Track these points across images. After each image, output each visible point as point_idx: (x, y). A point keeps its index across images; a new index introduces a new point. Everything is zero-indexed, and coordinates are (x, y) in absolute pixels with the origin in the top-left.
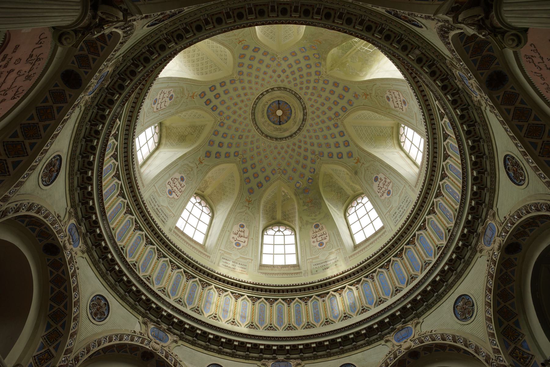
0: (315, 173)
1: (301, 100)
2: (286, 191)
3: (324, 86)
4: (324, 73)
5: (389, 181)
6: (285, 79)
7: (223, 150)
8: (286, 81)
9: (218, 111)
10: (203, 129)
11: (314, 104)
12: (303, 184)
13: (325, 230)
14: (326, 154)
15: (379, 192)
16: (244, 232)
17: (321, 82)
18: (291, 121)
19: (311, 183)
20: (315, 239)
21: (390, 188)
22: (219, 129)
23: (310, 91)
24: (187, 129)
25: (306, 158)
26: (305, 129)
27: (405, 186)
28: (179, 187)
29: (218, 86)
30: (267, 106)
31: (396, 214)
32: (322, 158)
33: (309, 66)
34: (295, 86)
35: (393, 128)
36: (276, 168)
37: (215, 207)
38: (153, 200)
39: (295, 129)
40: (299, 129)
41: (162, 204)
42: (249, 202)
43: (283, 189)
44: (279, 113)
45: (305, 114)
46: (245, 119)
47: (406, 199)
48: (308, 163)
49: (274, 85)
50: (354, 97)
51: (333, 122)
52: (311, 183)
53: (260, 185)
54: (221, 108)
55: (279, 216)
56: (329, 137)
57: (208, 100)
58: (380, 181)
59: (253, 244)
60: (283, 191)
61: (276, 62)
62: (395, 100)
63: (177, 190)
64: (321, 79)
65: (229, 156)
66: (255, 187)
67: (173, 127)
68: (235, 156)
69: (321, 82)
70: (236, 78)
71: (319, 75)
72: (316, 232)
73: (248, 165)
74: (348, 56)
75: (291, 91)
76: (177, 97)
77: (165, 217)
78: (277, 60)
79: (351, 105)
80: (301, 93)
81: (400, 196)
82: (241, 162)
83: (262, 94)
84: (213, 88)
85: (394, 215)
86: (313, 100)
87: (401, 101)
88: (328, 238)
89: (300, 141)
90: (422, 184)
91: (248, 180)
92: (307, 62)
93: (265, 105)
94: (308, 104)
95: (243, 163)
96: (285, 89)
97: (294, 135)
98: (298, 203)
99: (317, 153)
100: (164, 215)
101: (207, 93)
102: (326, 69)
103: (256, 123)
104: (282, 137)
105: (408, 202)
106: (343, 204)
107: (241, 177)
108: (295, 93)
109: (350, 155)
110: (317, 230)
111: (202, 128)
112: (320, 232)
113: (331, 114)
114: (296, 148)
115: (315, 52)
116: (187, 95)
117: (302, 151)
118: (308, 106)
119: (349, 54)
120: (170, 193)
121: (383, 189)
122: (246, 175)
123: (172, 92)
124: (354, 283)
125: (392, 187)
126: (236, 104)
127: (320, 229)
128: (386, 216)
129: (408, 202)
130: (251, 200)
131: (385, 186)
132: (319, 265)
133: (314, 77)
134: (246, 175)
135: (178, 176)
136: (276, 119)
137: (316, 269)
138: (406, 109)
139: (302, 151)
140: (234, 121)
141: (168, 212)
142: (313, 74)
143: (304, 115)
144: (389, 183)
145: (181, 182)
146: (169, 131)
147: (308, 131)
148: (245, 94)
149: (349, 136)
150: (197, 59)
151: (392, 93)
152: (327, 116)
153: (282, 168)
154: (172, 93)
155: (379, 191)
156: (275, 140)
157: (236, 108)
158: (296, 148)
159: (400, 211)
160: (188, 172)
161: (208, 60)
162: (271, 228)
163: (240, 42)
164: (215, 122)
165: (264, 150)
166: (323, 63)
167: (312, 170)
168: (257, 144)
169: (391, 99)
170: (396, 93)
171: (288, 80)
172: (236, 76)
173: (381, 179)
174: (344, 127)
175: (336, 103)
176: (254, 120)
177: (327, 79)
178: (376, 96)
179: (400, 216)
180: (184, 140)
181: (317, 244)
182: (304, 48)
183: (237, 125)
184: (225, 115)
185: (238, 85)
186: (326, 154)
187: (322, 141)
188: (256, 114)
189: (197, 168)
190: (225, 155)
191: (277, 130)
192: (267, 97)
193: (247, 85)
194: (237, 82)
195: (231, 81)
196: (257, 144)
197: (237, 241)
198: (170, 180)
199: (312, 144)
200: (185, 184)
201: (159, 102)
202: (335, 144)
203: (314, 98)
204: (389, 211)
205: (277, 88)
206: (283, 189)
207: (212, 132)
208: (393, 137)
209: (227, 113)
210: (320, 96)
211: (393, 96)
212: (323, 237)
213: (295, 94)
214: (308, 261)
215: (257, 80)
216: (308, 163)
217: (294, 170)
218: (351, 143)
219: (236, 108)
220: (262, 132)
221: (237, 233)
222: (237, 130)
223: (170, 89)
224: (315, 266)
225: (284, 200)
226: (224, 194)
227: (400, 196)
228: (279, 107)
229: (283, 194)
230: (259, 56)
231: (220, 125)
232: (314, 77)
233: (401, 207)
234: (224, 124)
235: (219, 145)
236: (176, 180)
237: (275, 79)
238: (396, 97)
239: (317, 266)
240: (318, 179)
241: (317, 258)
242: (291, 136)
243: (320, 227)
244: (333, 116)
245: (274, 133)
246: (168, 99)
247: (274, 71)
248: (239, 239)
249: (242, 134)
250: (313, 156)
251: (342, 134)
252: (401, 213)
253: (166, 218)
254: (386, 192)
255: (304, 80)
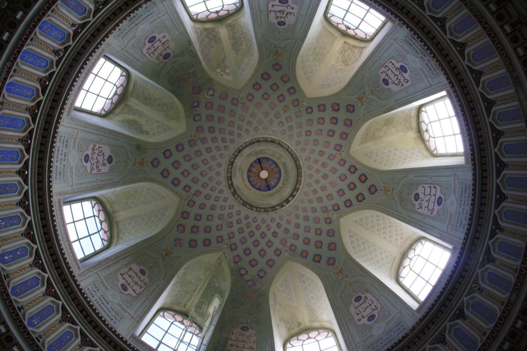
0: (192, 116)
1: (242, 203)
2: (225, 76)
3: (219, 233)
4: (226, 251)
5: (94, 172)
6: (270, 224)
7: (329, 114)
8: (268, 222)
9: (347, 165)
10: (363, 138)
11: (224, 203)
12: (204, 96)
13: (153, 58)
14: (187, 146)
15: (99, 147)
16: (277, 17)
17: (226, 237)
18: (246, 168)
19: (193, 102)
20: (163, 40)
21: (88, 165)
22: (341, 142)
23: (235, 219)
24: (384, 133)
25: (212, 129)
26: (225, 166)
27: (72, 186)
28: (389, 73)
29: (354, 201)
30: (282, 179)
31: (65, 146)
32: (190, 138)
33: (247, 252)
34: (255, 218)
35: (114, 212)
36: (248, 103)
37: (323, 26)
38: (432, 69)
39: (238, 162)
40: (232, 163)
41: (417, 60)
42: (277, 54)
43: (230, 78)
44: (264, 174)
45: (231, 186)
46: (308, 159)
47: (62, 175)
48: (206, 125)
49: (281, 211)
50: (180, 240)
51: (193, 191)
52: (195, 101)
53: (266, 76)
54: (343, 170)
55: (223, 31)
56: (191, 170)
57: (364, 182)
58: (104, 162)
59: (259, 5)
60: (228, 74)
61: (288, 245)
62: (136, 279)
63: (393, 70)
64: (227, 241)
65: (319, 106)
66: (272, 72)
67: (402, 131)
68: (311, 108)
69: (226, 237)
70: (333, 214)
71: (231, 245)
72: (165, 49)
73: (289, 99)
74: (206, 280)
75: (258, 209)
76: (408, 194)
77: (411, 43)
78: (288, 249)
79: (178, 226)
80: (245, 211)
81: (72, 168)
82: (300, 100)
83: (292, 195)
84: (360, 198)
85: (67, 141)
86: (227, 208)
87: (129, 284)
88: (145, 51)
89: (226, 148)
90: (60, 237)
91: (285, 79)
92: (251, 257)
93: (286, 180)
94: (231, 200)
95: (297, 100)
96: (266, 210)
97: (236, 154)
98: (203, 71)
99: (198, 142)
100: (412, 44)
101: (368, 192)
102: (226, 257)
103: (292, 155)
104: (251, 146)
105: (58, 174)
106: (135, 84)
107: (297, 82)
108: (252, 210)
109: (155, 163)
110: (164, 53)
111: (364, 140)
112: (159, 51)
113: (199, 200)
114: (229, 137)
115: (247, 277)
116: (394, 193)
117: (220, 137)
118: (231, 198)
119: (205, 282)
120: (403, 69)
121: (95, 156)
122: (289, 85)
123: (417, 206)
124: (82, 29)
125: (86, 170)
126: (325, 177)
127: (161, 55)
128: (76, 131)
129: (58, 174)
130: (275, 57)
131: (95, 161)
132: (145, 16)
133: (236, 239)
134: (289, 85)
135: (391, 86)
136: (265, 164)
137: (147, 10)
138: (119, 281)
139: (220, 137)
140: (321, 153)
141: (405, 46)
142: (239, 244)
143: (232, 184)
144: (92, 169)
145: (387, 78)
146: (407, 125)
147: (219, 165)
148: (315, 191)
149: (165, 186)
150: (386, 229)
151: (143, 285)
152: (203, 195)
153: (240, 105)
154: (417, 203)
155: (100, 149)
156: (261, 139)
157: (324, 171)
158: (229, 137)
159: (62, 154)
160: (377, 89)
161: (372, 230)
162: (231, 12)
163: (340, 271)
164: (349, 150)
165: (271, 122)
166: (232, 265)
167: (197, 118)
168: (283, 128)
169: (139, 275)
170: (138, 290)
171: (266, 224)
172: (334, 216)
173: (104, 165)
174: (177, 194)
175: (198, 217)
176: (295, 160)
177: (220, 244)
178: (156, 262)
179: (59, 149)
180: (387, 120)
181: (158, 37)
182: (262, 277)
183: (318, 148)
184: (336, 160)
185: (329, 204)
186: (187, 146)
187: (198, 160)
188: (294, 167)
189: (364, 93)
190: (325, 108)
191: (261, 152)
192: (286, 193)
193: (316, 204)
194: (330, 208)
195: (339, 209)
196: (283, 128)
197: (286, 5)
198: (405, 85)
199: (208, 150)
200: (381, 75)
201: (433, 198)
202: (179, 164)
203: (227, 211)
204: (75, 139)
205: (277, 209)
206: (230, 78)
207: (349, 137)
208: (109, 202)
209: (334, 164)
210: (221, 217)
211: (140, 283)
212: (153, 49)
213: (251, 207)
214: (164, 12)
215: (305, 214)
216: (206, 125)
217: (222, 109)
218: (160, 178)
219: (324, 171)
220: (281, 146)
221: (287, 14)
222: (316, 142)
223: (419, 210)
224: (151, 11)
225: (223, 61)
226: (314, 49)
227: (72, 168)
228: (267, 182)
229: (227, 71)
230: (312, 250)
231: (341, 146)
232: (236, 239)
233: (63, 161)
234: (335, 149)
235: (337, 121)
236: (396, 82)
237: (282, 220)
238: (136, 283)
239: (148, 13)
240: (185, 111)
241: (151, 23)
242: (240, 151)
243: (161, 58)
244: (195, 198)
245: (263, 148)
246: (421, 196)
247: (286, 231)
248: (282, 8)
249: (308, 138)
250: (202, 135)
251: (176, 182)
252: (60, 154)
253: (408, 40)
254: (90, 156)
255: (247, 231)
